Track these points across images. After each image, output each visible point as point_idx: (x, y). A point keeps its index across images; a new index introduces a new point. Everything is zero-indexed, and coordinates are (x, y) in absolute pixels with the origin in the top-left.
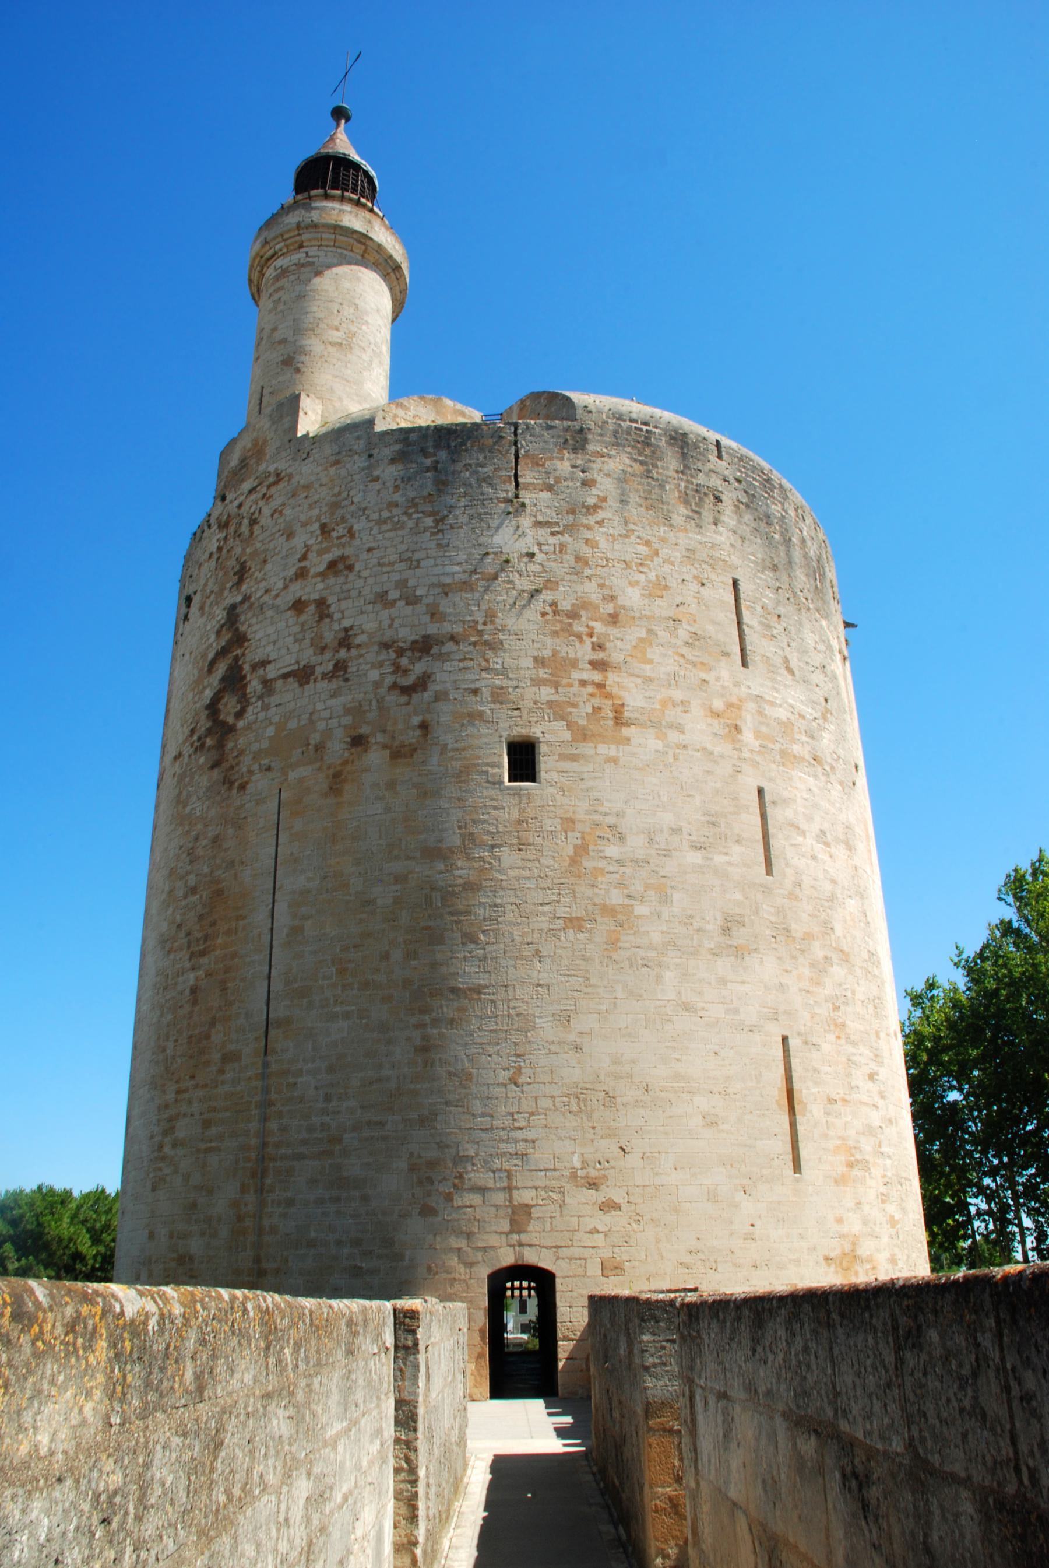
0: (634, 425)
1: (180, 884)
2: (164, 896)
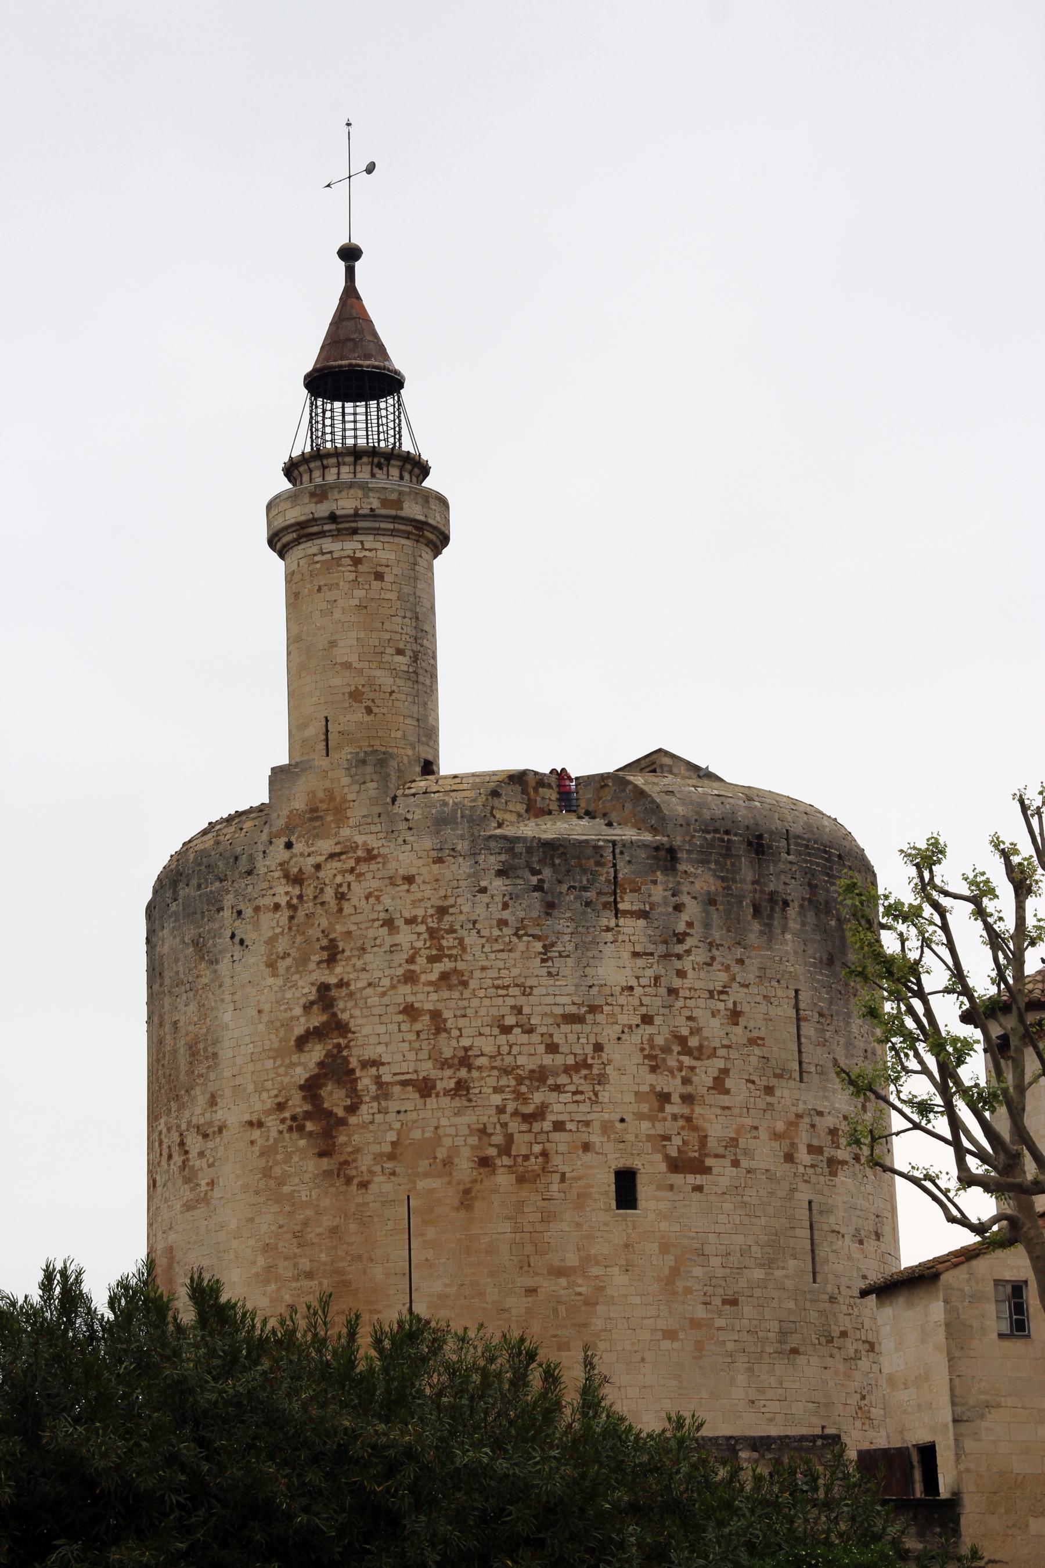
0: (718, 835)
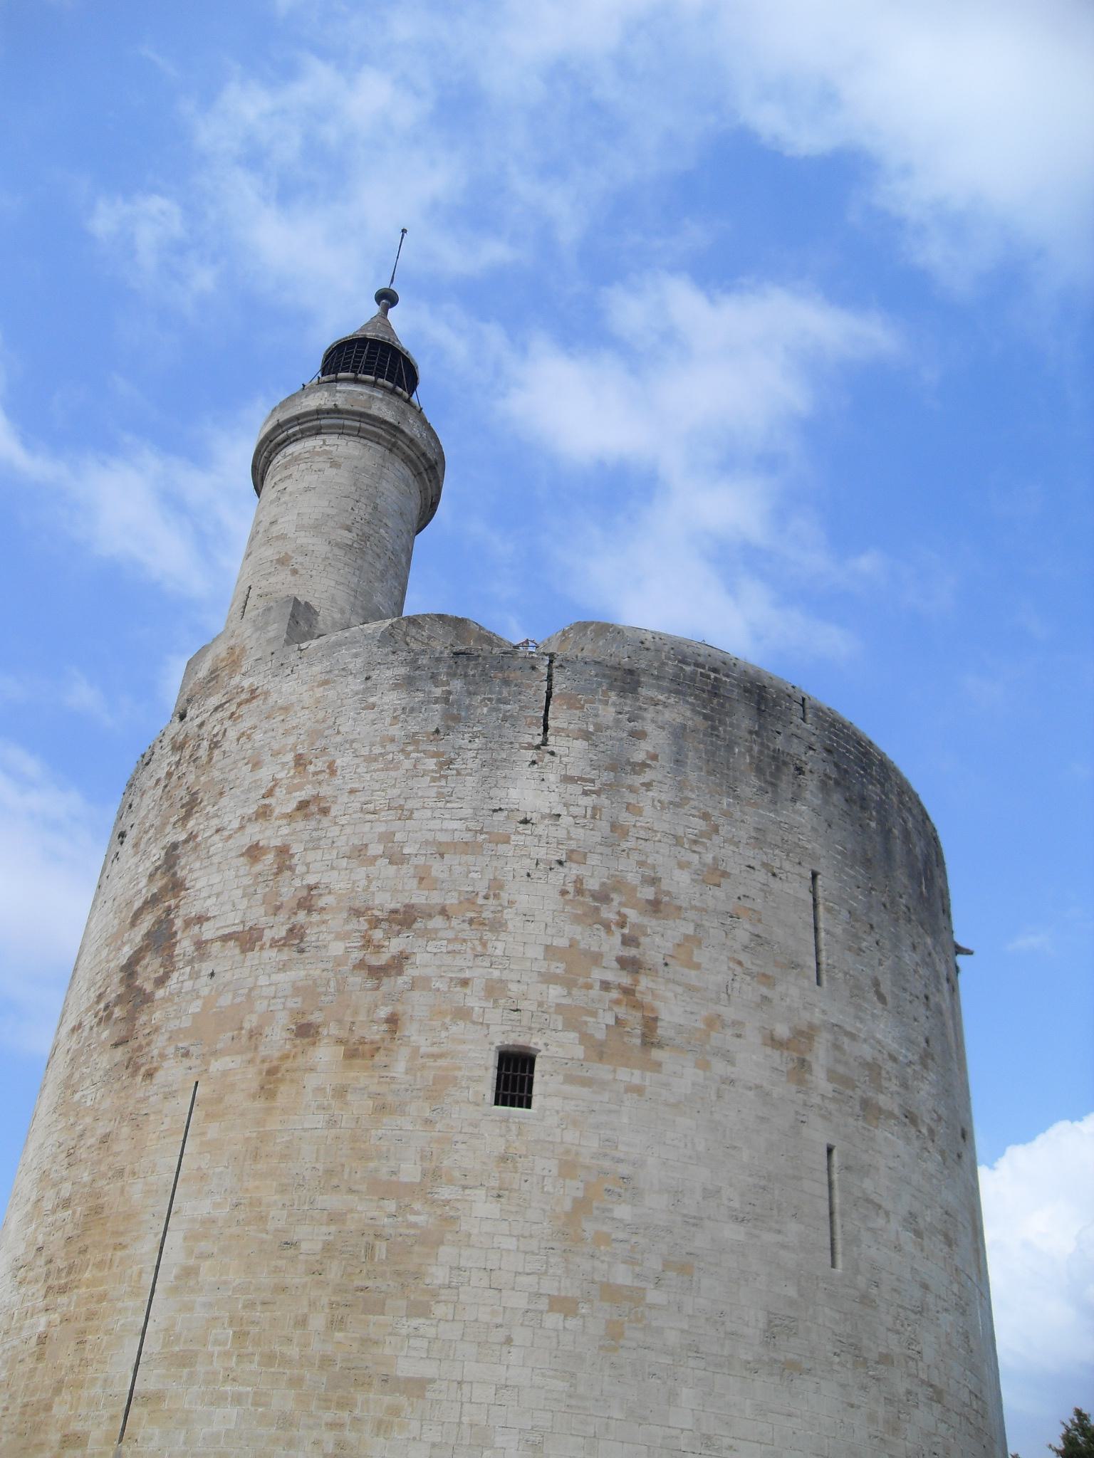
1: (50, 1193)
2: (29, 1207)
